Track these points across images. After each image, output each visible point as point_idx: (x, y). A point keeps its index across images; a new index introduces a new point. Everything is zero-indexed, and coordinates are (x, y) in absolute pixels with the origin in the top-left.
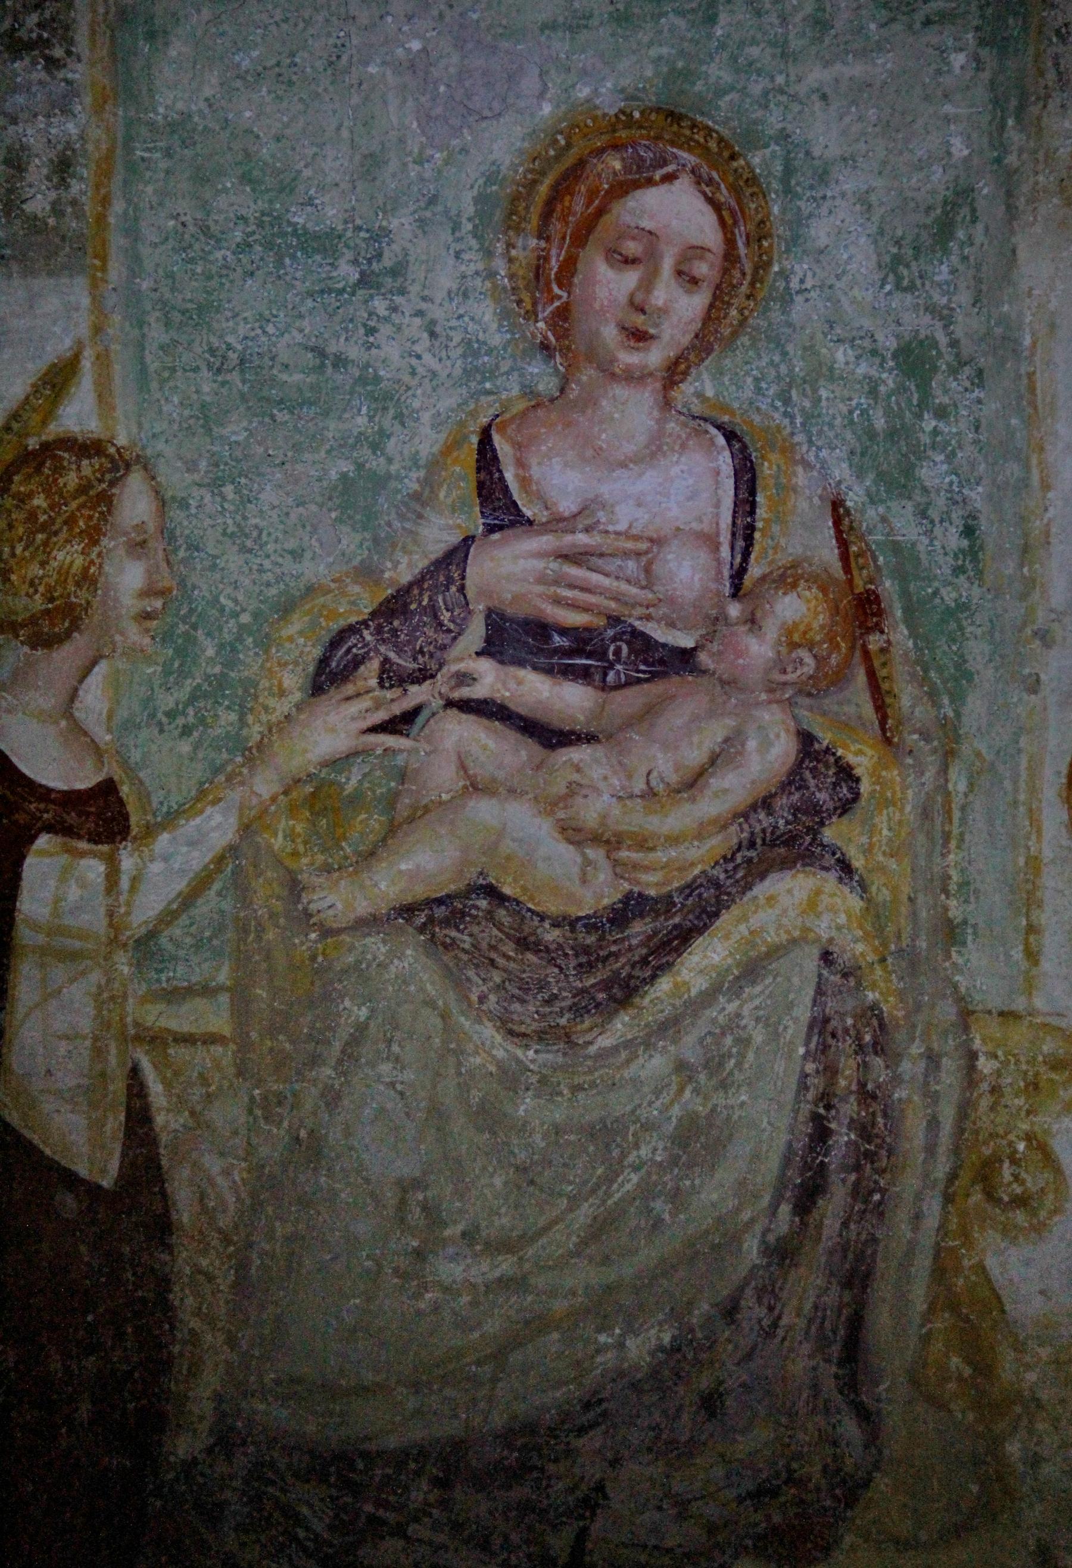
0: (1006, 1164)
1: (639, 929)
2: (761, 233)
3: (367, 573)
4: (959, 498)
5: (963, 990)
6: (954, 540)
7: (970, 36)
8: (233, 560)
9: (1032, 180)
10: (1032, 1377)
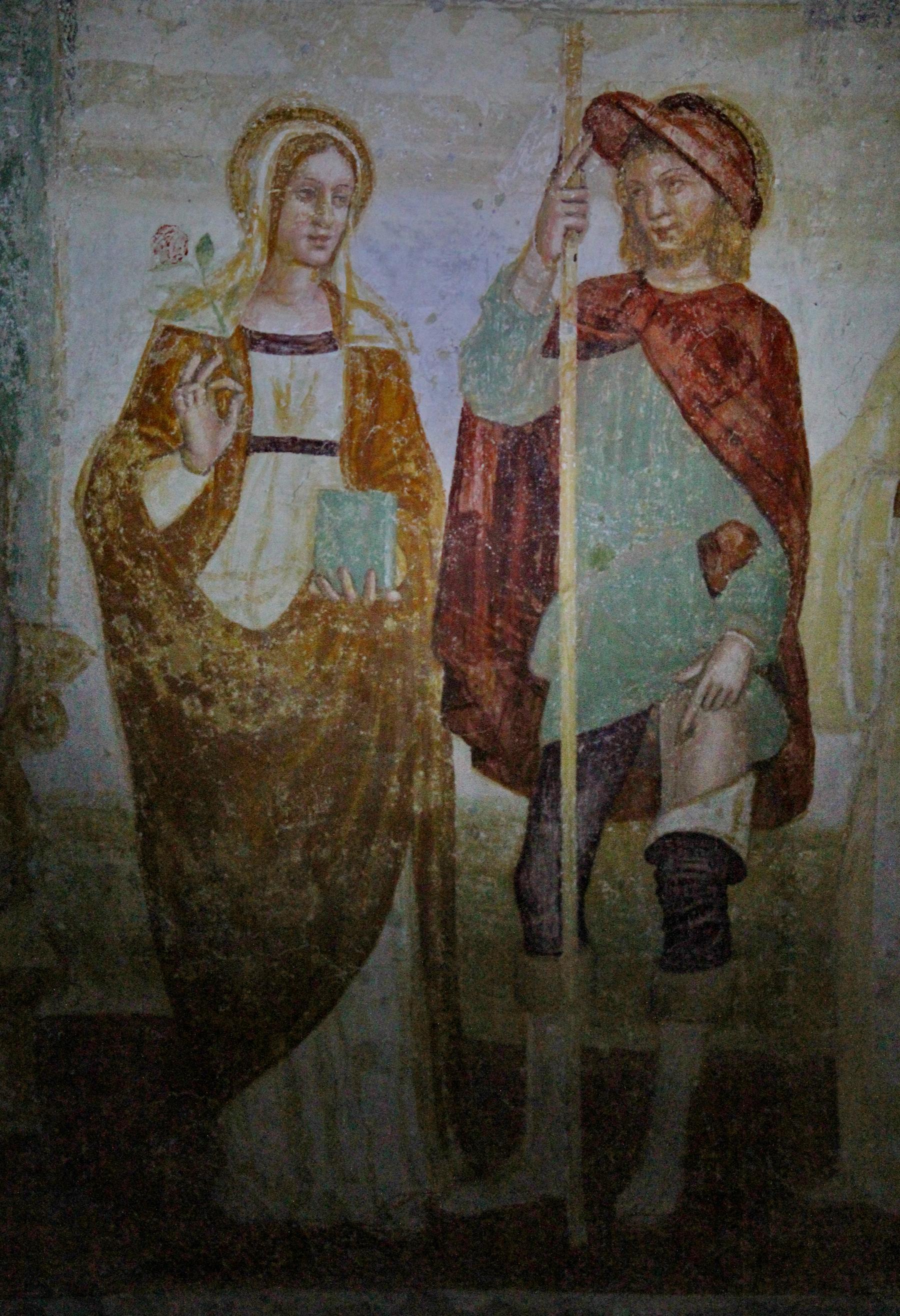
0: (35, 707)
4: (15, 332)
5: (12, 610)
6: (12, 356)
7: (19, 69)
9: (55, 154)
10: (43, 826)
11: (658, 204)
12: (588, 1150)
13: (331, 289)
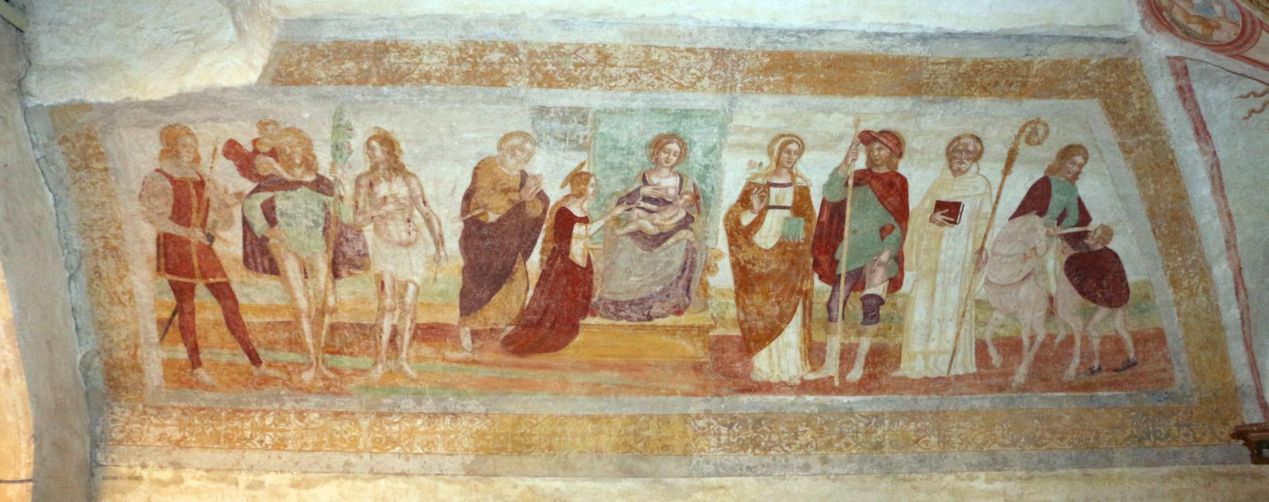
1: (662, 237)
2: (686, 149)
3: (625, 190)
8: (606, 188)
11: (876, 153)
12: (840, 365)
13: (792, 173)
